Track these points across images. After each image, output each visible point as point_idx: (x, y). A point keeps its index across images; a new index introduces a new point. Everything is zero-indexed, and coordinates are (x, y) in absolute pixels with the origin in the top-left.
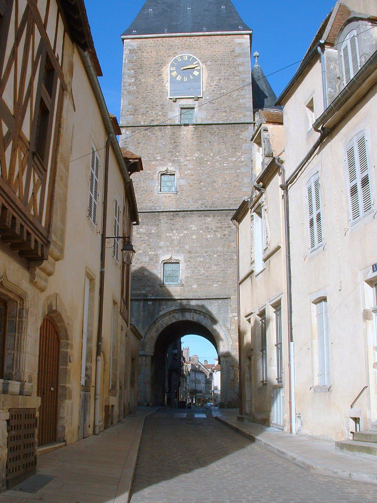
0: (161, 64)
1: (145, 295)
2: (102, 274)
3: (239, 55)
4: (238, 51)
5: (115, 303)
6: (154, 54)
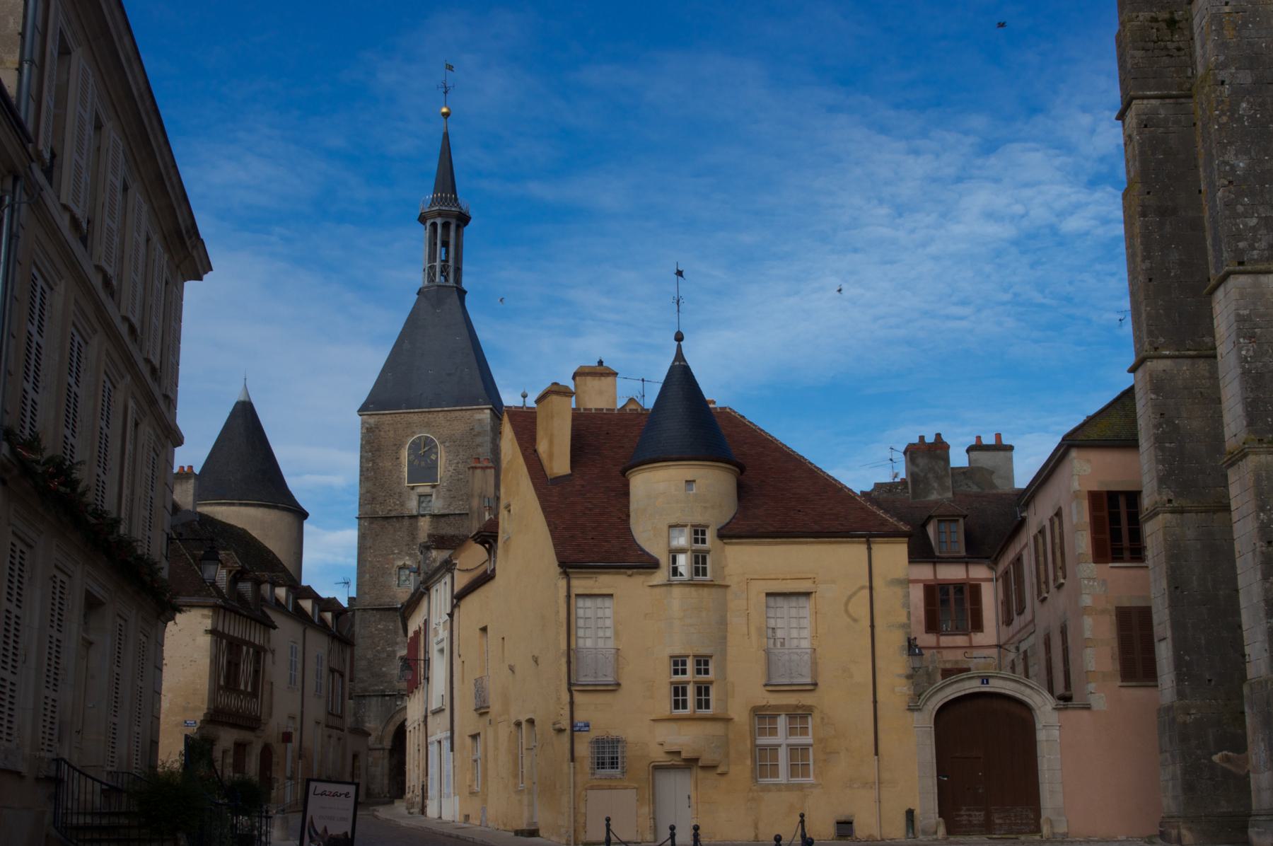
0: (399, 446)
1: (383, 691)
2: (302, 712)
3: (479, 434)
4: (477, 429)
5: (318, 723)
6: (391, 434)
